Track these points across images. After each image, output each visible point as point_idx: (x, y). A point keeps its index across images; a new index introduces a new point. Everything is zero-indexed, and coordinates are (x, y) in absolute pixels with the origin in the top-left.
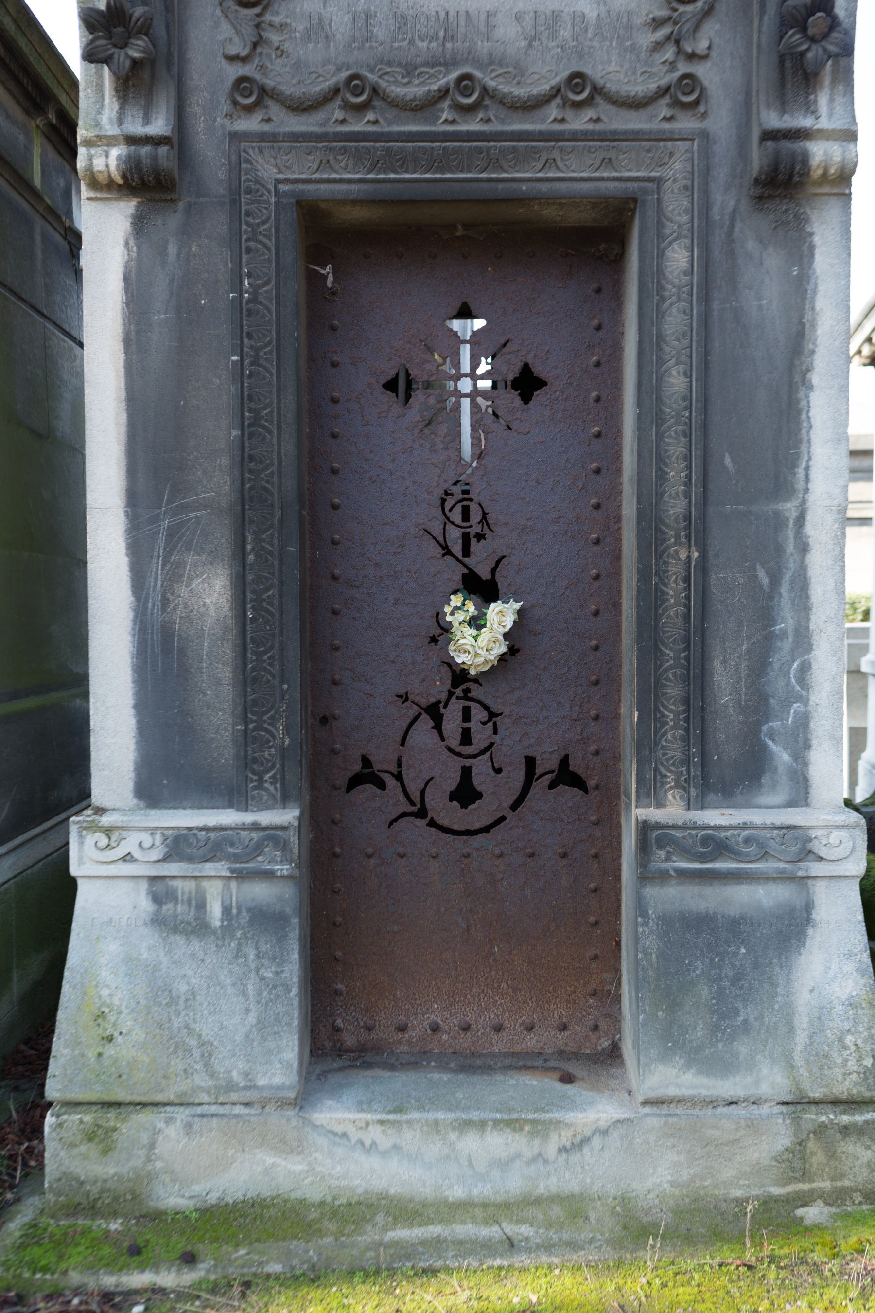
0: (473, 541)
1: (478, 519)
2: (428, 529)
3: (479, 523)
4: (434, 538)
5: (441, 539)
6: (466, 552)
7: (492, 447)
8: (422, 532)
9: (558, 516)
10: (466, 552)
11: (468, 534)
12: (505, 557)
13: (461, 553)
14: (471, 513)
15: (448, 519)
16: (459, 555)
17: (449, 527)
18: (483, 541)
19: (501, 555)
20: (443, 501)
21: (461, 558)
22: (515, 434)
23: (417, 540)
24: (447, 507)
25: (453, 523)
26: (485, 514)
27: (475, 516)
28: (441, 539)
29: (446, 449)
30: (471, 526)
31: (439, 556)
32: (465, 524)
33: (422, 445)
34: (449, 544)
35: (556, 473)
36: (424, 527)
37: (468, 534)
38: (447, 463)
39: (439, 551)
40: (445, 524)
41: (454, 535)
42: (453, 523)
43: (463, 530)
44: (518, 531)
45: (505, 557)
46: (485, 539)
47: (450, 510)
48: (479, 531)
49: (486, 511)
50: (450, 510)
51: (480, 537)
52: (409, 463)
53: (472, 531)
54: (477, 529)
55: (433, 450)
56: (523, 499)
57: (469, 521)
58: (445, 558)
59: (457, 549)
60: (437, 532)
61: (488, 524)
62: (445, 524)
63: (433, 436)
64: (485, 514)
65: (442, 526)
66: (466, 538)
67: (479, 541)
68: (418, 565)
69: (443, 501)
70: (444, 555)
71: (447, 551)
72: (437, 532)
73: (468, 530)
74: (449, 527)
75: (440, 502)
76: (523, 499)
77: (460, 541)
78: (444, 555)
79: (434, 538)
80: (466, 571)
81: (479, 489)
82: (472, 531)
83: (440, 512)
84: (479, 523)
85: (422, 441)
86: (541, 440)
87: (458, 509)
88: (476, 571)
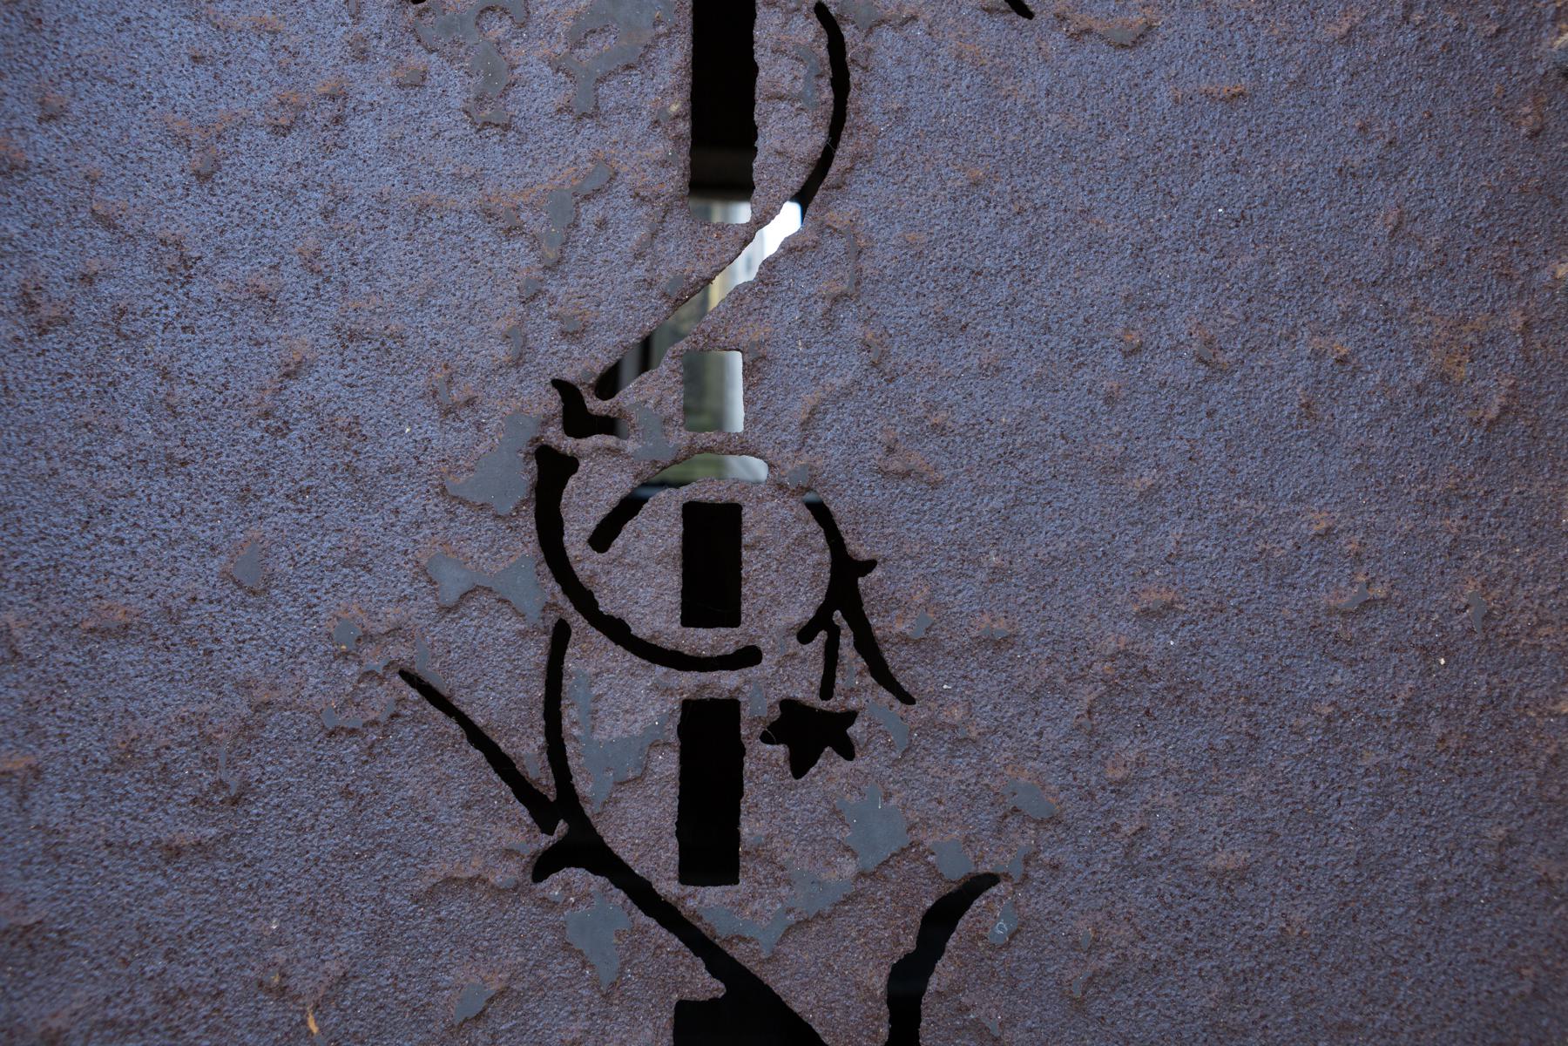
0: (763, 762)
1: (802, 610)
2: (432, 673)
3: (805, 635)
4: (476, 737)
5: (529, 751)
6: (710, 846)
7: (900, 115)
8: (388, 694)
9: (1349, 598)
10: (710, 846)
11: (728, 709)
12: (991, 879)
13: (670, 852)
14: (751, 564)
15: (583, 598)
16: (659, 863)
17: (590, 657)
18: (830, 764)
19: (956, 870)
20: (553, 471)
21: (668, 886)
22: (1057, 41)
23: (350, 750)
24: (582, 510)
25: (616, 630)
26: (846, 572)
27: (781, 584)
28: (529, 751)
29: (588, 114)
30: (748, 656)
31: (509, 873)
32: (706, 640)
33: (418, 81)
34: (583, 786)
35: (1334, 305)
36: (401, 652)
37: (728, 709)
38: (591, 213)
39: (521, 835)
40: (561, 636)
41: (626, 717)
42: (616, 630)
43: (689, 682)
44: (1086, 695)
45: (991, 879)
46: (847, 750)
47: (602, 538)
48: (804, 689)
49: (859, 549)
50: (602, 538)
51: (811, 733)
52: (318, 199)
53: (756, 694)
54: (785, 676)
55: (491, 118)
56: (1116, 467)
57: (731, 618)
58: (553, 886)
59: (643, 826)
60: (503, 697)
61: (868, 646)
62: (561, 636)
63: (498, 28)
64: (846, 572)
65: (536, 654)
66: (708, 738)
67: (800, 765)
68: (349, 943)
69: (553, 471)
70: (544, 866)
71: (571, 839)
72: (503, 697)
73: (727, 681)
74: (590, 657)
75: (525, 476)
76: (1116, 467)
77: (668, 764)
78: (544, 866)
79: (476, 737)
80: (705, 985)
81: (810, 396)
82: (756, 694)
83: (526, 545)
84: (805, 635)
85: (418, 59)
86: (1226, 86)
87: (658, 533)
88: (781, 984)
